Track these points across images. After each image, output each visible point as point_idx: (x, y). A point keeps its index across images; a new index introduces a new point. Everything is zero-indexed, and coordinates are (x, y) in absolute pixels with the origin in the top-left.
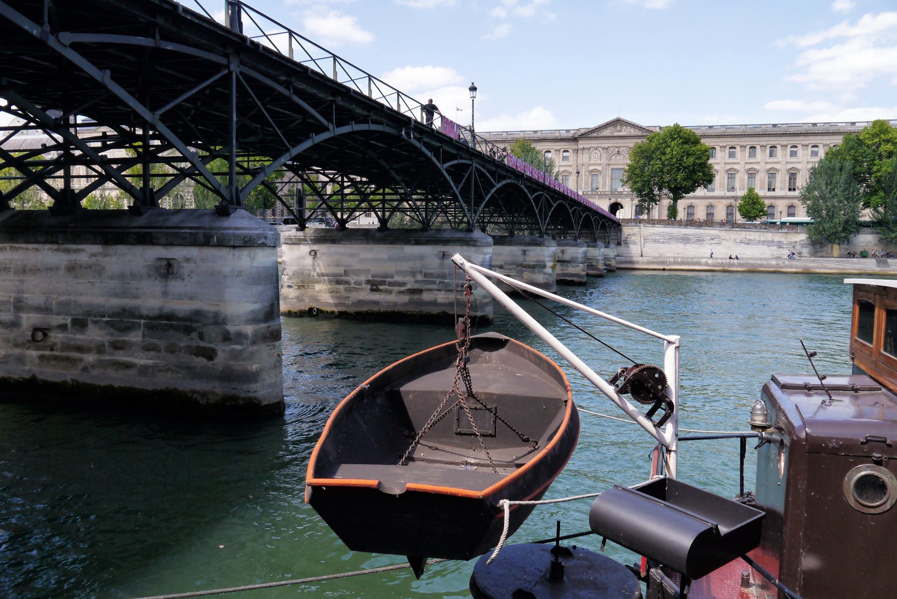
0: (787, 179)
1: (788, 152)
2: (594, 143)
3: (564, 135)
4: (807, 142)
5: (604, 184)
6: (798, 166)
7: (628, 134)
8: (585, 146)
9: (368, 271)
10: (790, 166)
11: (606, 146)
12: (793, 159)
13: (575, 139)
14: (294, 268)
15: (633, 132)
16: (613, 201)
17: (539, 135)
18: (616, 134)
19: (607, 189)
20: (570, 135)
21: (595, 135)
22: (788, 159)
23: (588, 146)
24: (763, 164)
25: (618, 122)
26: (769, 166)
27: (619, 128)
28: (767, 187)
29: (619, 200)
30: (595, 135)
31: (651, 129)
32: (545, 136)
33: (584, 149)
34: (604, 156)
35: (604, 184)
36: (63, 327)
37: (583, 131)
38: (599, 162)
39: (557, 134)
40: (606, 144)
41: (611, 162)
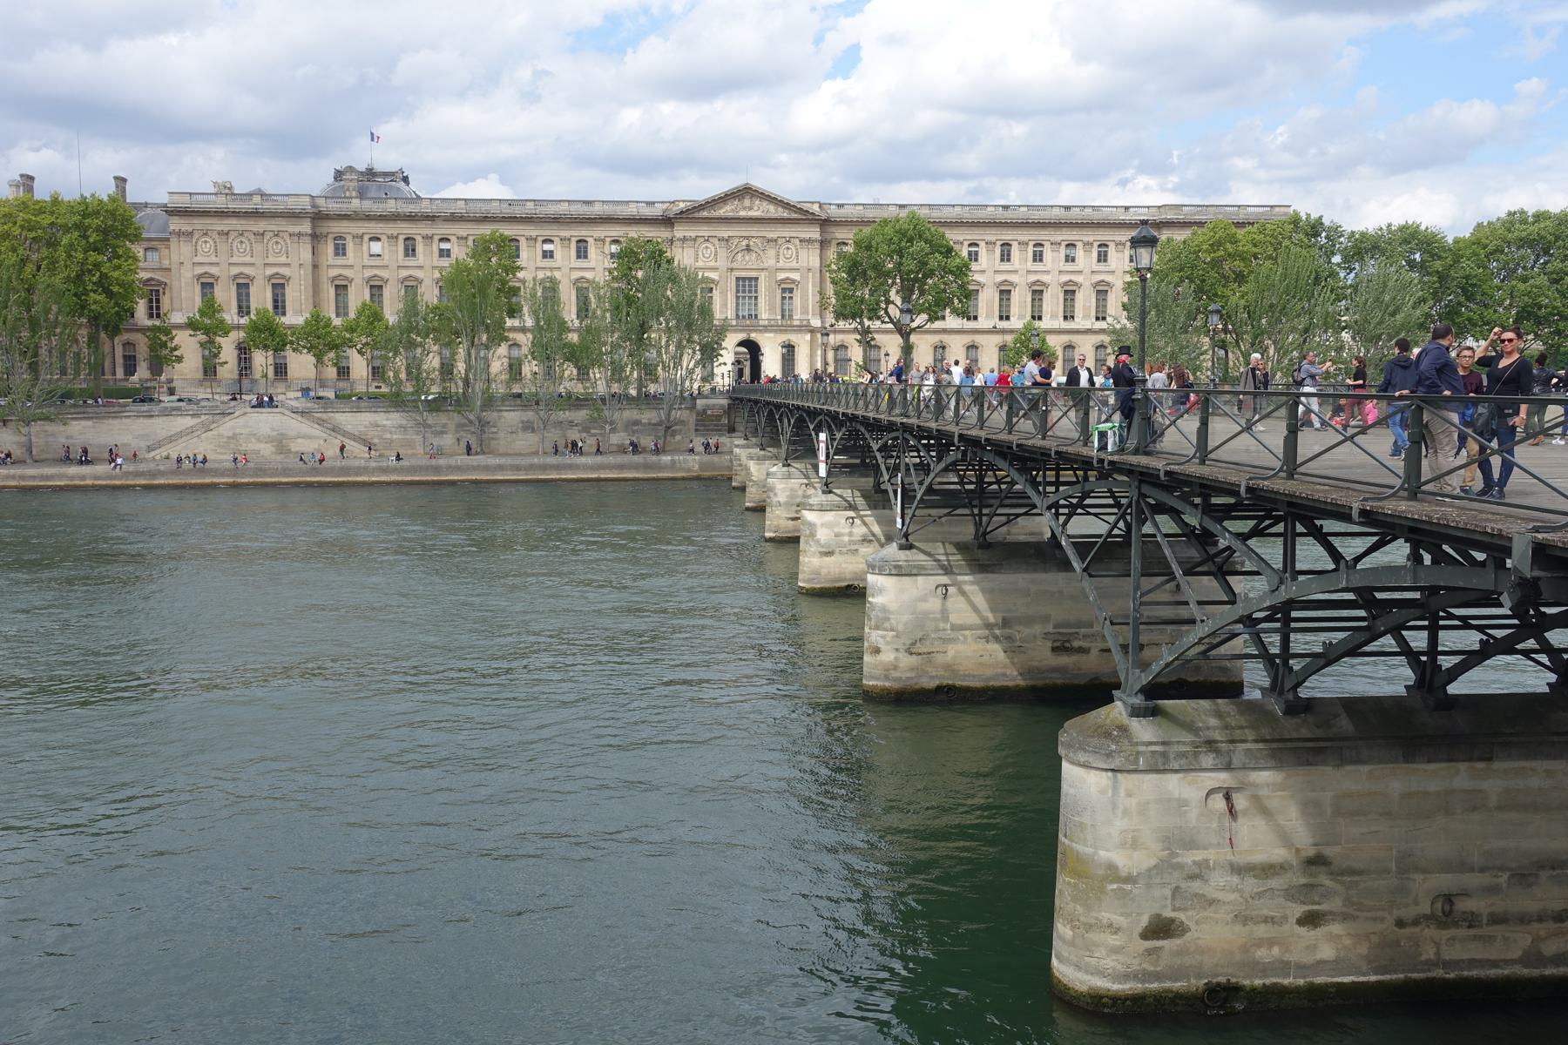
0: (1029, 299)
1: (1030, 255)
2: (704, 231)
3: (647, 212)
4: (1059, 239)
5: (725, 305)
6: (1045, 278)
7: (764, 215)
8: (688, 234)
9: (1045, 619)
10: (1033, 278)
11: (726, 235)
12: (1038, 267)
13: (667, 221)
14: (906, 617)
15: (773, 211)
16: (741, 336)
17: (597, 210)
18: (743, 213)
19: (730, 314)
20: (657, 211)
21: (705, 214)
22: (1030, 265)
23: (693, 235)
24: (990, 274)
25: (746, 192)
26: (1000, 278)
27: (747, 202)
28: (997, 313)
29: (753, 336)
30: (705, 214)
31: (806, 207)
32: (609, 210)
33: (684, 239)
34: (722, 253)
35: (725, 305)
36: (1493, 890)
37: (682, 205)
38: (712, 264)
39: (631, 210)
40: (725, 232)
41: (734, 265)
